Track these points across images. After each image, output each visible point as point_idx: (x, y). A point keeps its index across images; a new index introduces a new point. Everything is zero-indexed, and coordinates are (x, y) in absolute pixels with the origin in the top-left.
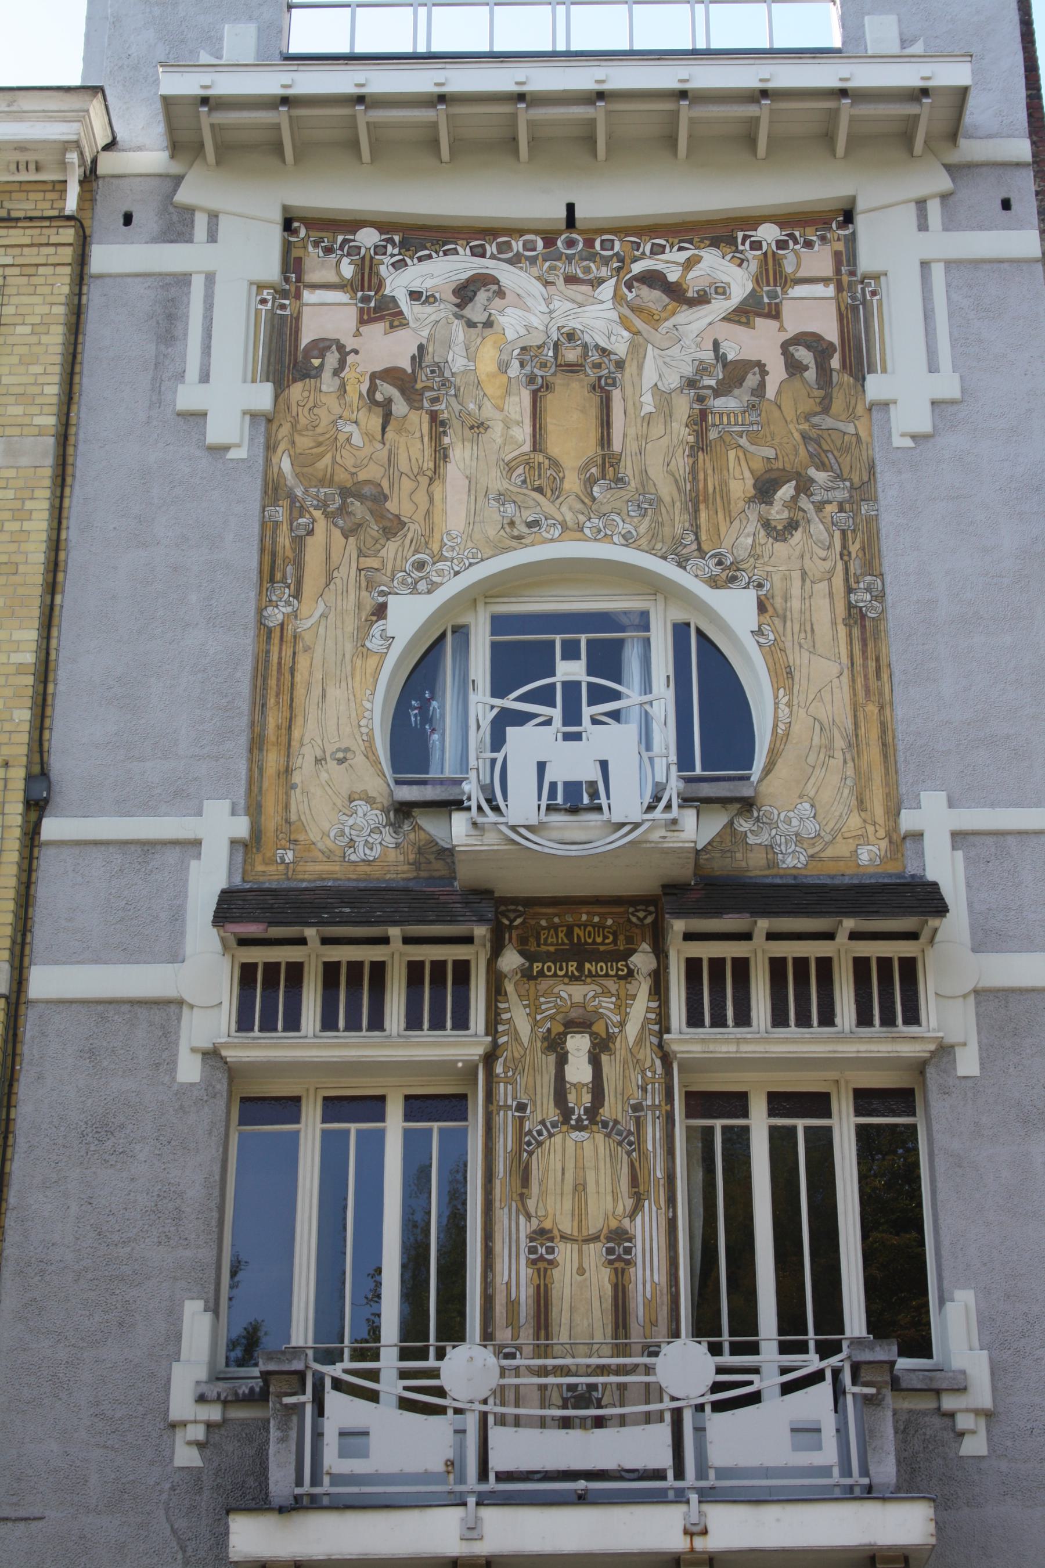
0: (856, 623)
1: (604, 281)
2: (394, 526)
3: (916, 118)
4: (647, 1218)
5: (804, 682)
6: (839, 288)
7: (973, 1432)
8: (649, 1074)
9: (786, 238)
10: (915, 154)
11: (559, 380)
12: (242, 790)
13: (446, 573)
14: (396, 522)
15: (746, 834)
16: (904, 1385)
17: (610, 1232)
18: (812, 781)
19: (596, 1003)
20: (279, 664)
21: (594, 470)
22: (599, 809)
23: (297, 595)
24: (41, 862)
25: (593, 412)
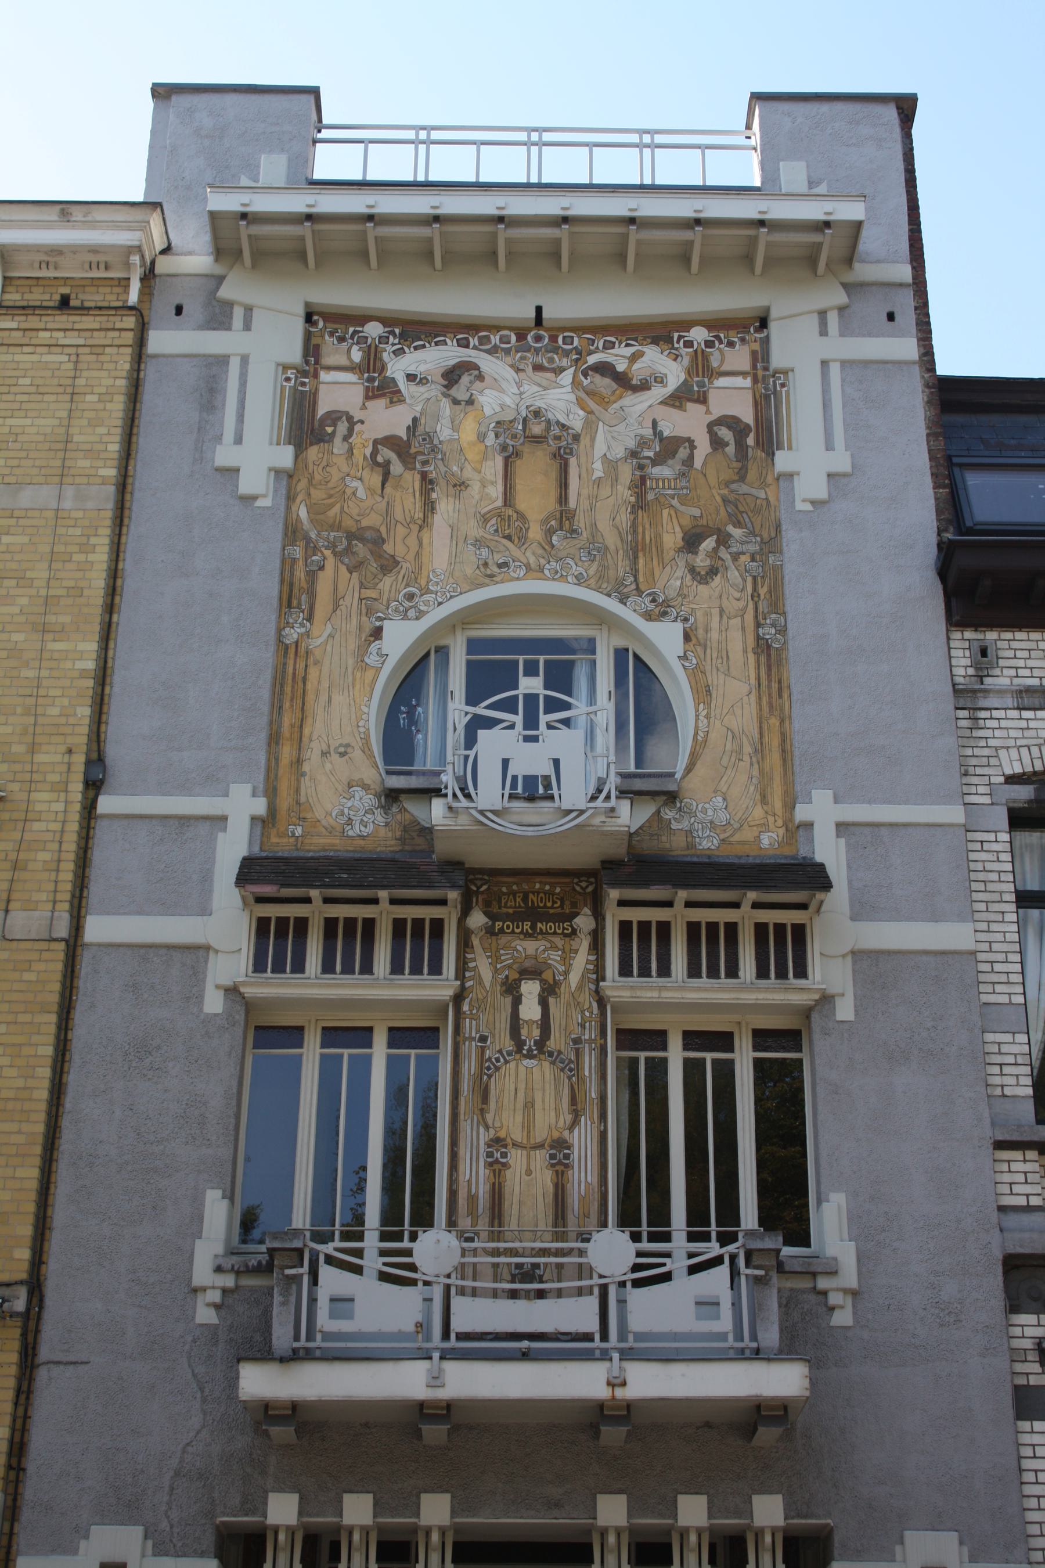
0: (763, 651)
1: (565, 370)
2: (389, 565)
3: (820, 244)
4: (583, 1131)
5: (720, 700)
6: (755, 381)
7: (842, 1307)
8: (587, 1014)
9: (713, 339)
10: (818, 274)
11: (526, 449)
12: (261, 777)
13: (431, 603)
16: (787, 1268)
17: (553, 1141)
18: (725, 779)
19: (546, 955)
20: (294, 674)
21: (553, 523)
22: (551, 798)
23: (310, 618)
24: (97, 831)
25: (554, 474)
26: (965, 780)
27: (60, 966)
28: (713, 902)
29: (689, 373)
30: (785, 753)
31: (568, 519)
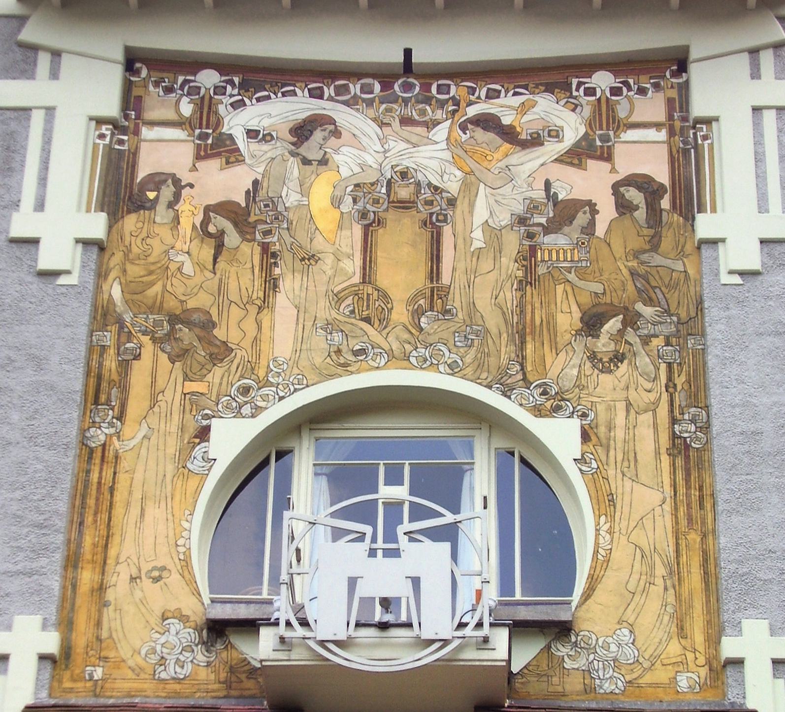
0: (680, 453)
1: (439, 123)
5: (626, 509)
6: (671, 133)
9: (621, 85)
11: (391, 216)
12: (53, 608)
13: (270, 396)
14: (222, 349)
15: (563, 659)
18: (631, 607)
20: (99, 483)
21: (422, 302)
23: (121, 417)
25: (423, 247)
29: (590, 125)
30: (710, 578)
31: (441, 298)
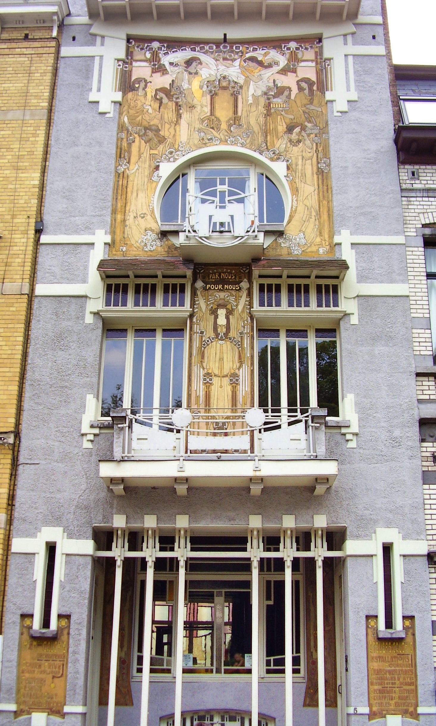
0: (320, 174)
1: (236, 60)
5: (302, 193)
6: (317, 64)
7: (352, 440)
11: (220, 92)
17: (231, 374)
20: (122, 185)
21: (231, 122)
22: (230, 232)
23: (129, 163)
26: (405, 226)
27: (25, 305)
28: (299, 276)
